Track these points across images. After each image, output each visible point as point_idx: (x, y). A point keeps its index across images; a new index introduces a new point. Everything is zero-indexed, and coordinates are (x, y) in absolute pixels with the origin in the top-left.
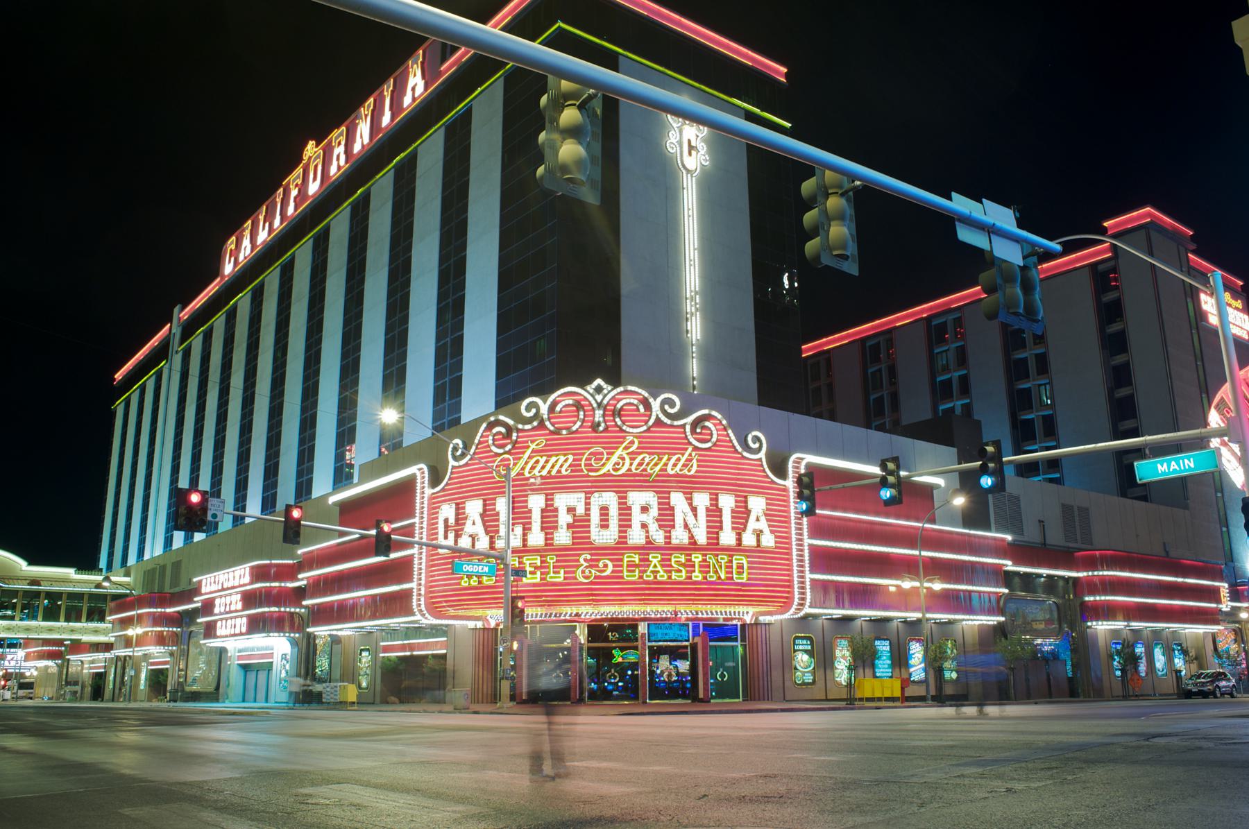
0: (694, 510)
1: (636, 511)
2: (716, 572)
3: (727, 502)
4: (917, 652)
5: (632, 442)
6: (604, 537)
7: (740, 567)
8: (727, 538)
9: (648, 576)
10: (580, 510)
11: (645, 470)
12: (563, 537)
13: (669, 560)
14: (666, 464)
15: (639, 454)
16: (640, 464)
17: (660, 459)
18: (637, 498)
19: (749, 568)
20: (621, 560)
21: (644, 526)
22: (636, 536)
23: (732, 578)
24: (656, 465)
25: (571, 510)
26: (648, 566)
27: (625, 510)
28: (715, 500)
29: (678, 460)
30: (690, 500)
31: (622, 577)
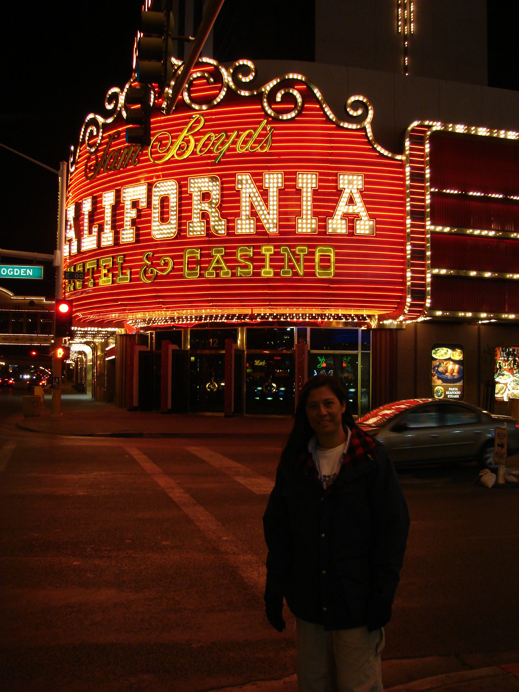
0: (264, 193)
1: (196, 198)
2: (292, 267)
3: (307, 181)
4: (57, 379)
5: (198, 121)
6: (162, 231)
7: (325, 259)
8: (306, 225)
9: (210, 274)
10: (143, 204)
11: (210, 151)
12: (128, 235)
13: (234, 254)
14: (234, 143)
15: (204, 133)
16: (205, 145)
17: (228, 137)
18: (200, 184)
19: (337, 261)
20: (181, 257)
21: (205, 216)
22: (196, 228)
23: (314, 274)
24: (223, 144)
25: (135, 204)
26: (209, 262)
27: (184, 198)
28: (290, 179)
29: (250, 136)
30: (258, 181)
31: (182, 276)
